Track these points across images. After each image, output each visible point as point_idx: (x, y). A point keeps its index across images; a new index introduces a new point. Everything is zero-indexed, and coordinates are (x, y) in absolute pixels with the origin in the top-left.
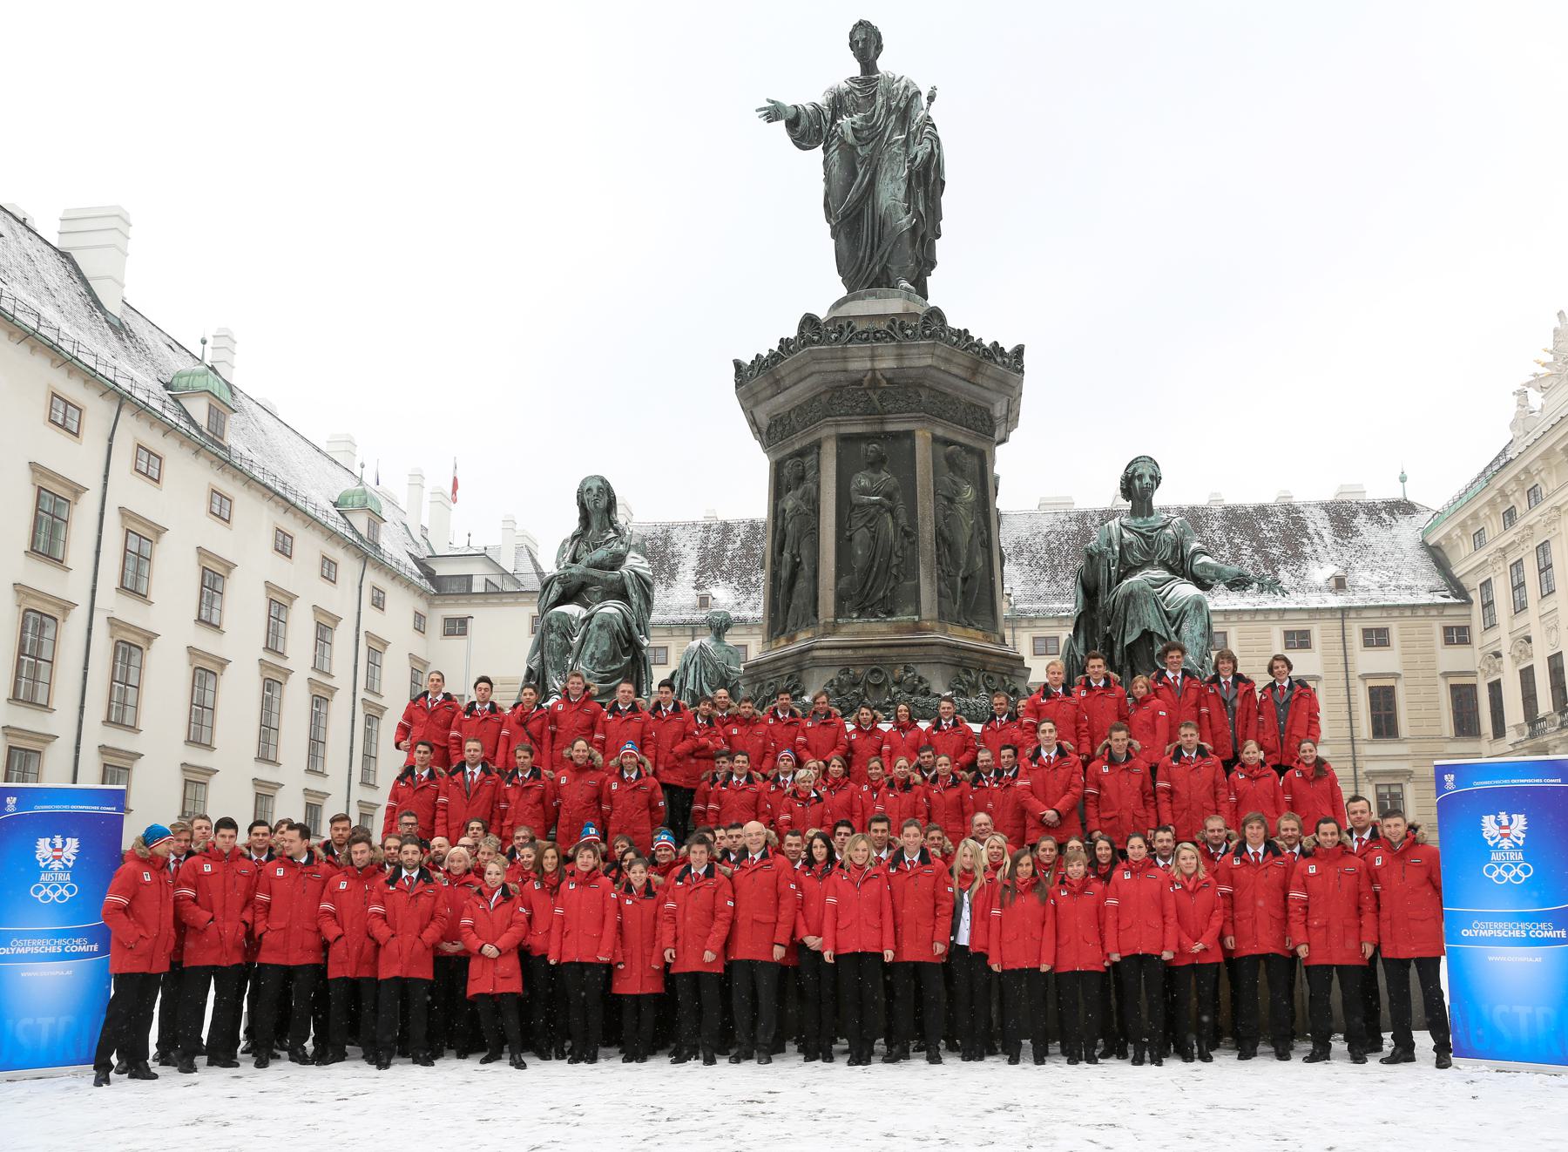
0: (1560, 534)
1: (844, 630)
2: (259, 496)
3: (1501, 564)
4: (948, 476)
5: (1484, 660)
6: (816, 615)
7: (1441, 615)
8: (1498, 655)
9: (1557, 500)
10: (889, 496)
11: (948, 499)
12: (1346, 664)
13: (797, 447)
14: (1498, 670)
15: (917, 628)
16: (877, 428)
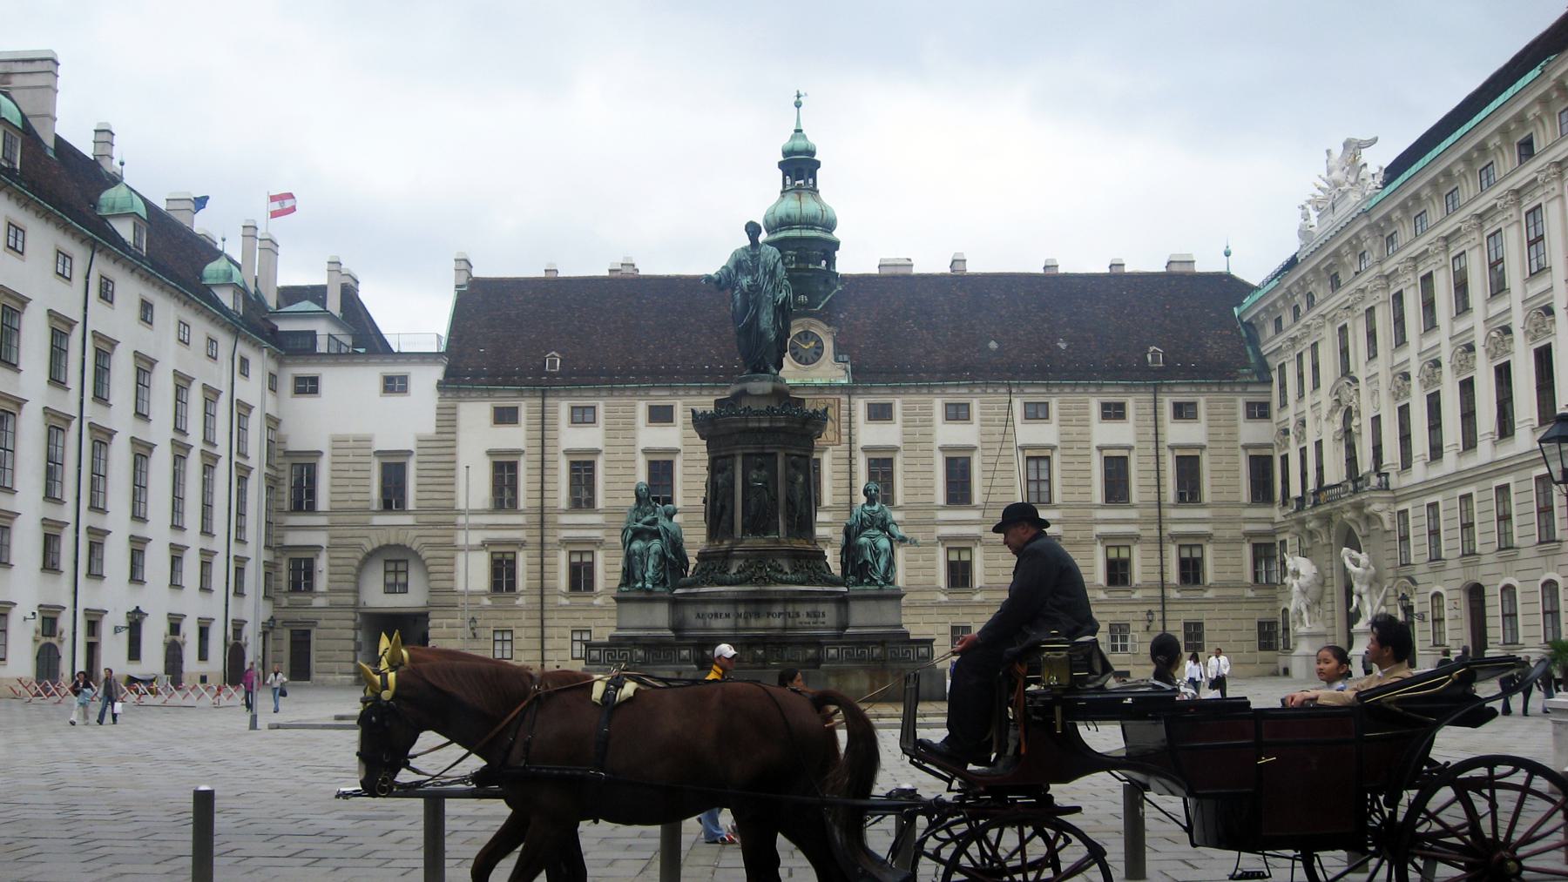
0: (1324, 338)
1: (746, 542)
2: (168, 295)
3: (1291, 353)
4: (792, 471)
5: (1277, 435)
6: (733, 533)
7: (1244, 392)
8: (1286, 432)
9: (1558, 153)
10: (765, 483)
11: (791, 481)
12: (1157, 434)
13: (723, 453)
14: (1287, 446)
15: (777, 541)
16: (760, 451)
